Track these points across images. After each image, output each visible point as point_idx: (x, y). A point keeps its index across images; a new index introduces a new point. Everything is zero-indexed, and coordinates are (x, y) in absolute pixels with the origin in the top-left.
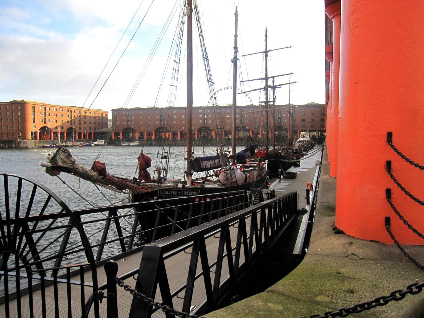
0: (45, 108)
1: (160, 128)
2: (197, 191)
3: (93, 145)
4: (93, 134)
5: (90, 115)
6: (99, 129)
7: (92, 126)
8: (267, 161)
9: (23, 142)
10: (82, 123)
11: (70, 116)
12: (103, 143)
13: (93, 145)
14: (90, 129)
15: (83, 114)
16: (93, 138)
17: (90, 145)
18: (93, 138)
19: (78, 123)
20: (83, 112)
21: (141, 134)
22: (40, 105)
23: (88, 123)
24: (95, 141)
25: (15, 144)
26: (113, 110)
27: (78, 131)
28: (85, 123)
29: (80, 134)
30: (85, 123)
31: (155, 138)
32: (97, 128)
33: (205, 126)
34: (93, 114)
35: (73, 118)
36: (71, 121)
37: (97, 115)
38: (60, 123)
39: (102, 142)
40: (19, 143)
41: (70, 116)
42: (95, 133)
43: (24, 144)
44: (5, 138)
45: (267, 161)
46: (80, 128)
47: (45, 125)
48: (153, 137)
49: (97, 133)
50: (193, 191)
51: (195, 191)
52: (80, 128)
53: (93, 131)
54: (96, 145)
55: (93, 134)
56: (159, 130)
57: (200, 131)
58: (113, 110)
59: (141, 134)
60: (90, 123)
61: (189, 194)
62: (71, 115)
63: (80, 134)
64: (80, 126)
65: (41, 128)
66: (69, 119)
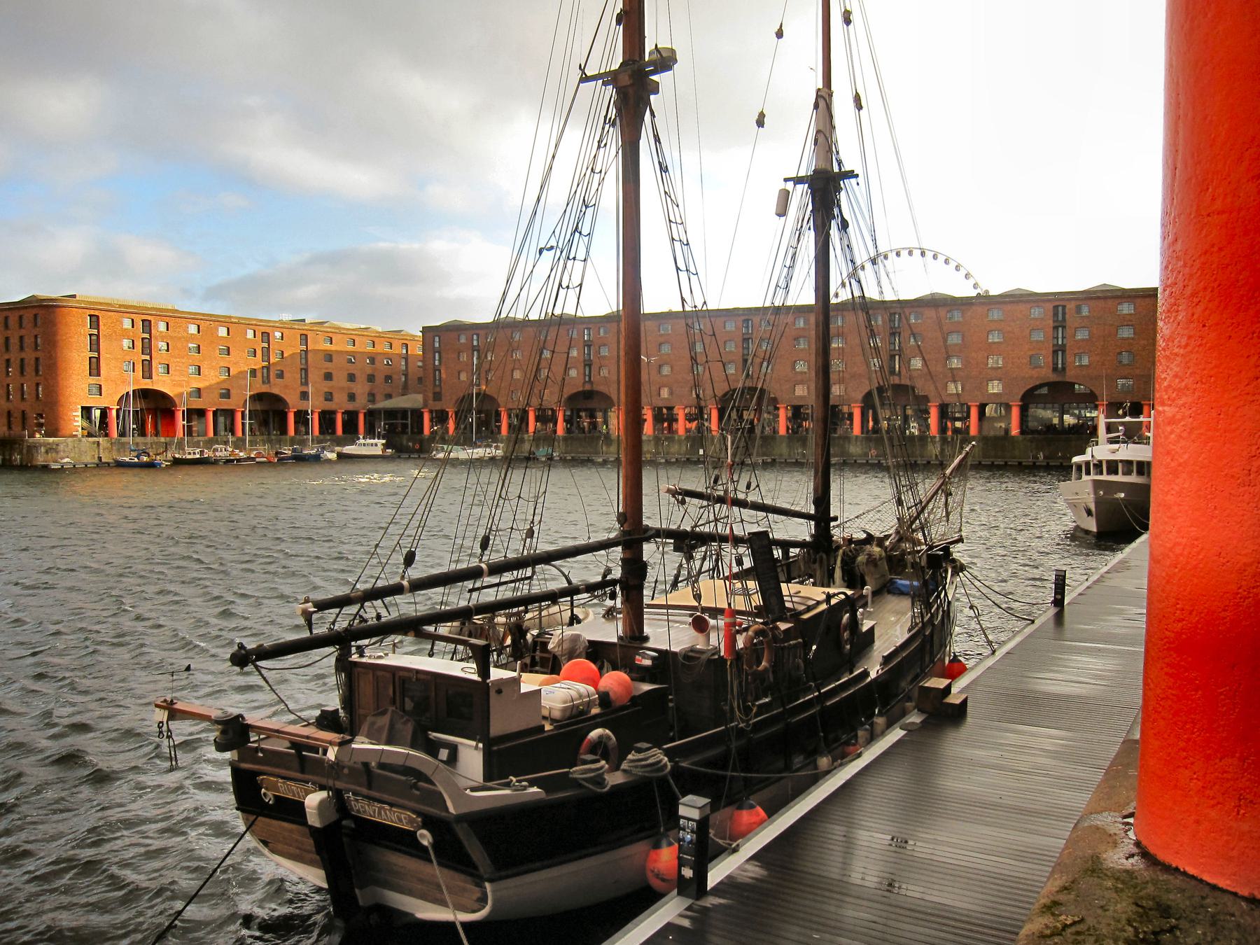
0: (147, 325)
4: (361, 417)
6: (389, 396)
9: (45, 444)
10: (315, 376)
11: (259, 353)
12: (378, 451)
13: (332, 456)
14: (352, 397)
17: (316, 458)
22: (125, 310)
25: (21, 453)
26: (426, 330)
28: (328, 376)
30: (328, 376)
31: (569, 431)
32: (378, 397)
34: (364, 347)
37: (383, 348)
38: (212, 377)
39: (375, 446)
40: (33, 448)
41: (259, 353)
43: (47, 452)
46: (304, 395)
47: (147, 384)
49: (378, 411)
53: (361, 405)
54: (341, 456)
55: (361, 417)
56: (586, 403)
58: (426, 330)
60: (352, 378)
64: (304, 389)
66: (258, 363)
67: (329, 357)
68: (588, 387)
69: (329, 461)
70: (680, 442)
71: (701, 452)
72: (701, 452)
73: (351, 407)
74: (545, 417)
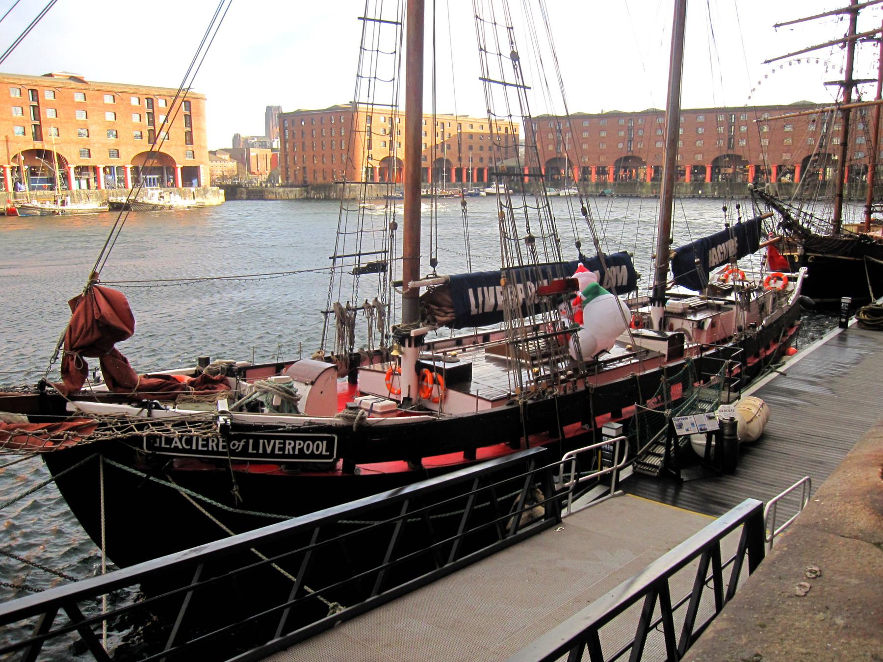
1: (626, 158)
2: (322, 439)
3: (483, 194)
5: (481, 131)
7: (486, 154)
8: (803, 270)
13: (483, 194)
14: (481, 160)
15: (466, 129)
16: (485, 180)
17: (477, 195)
18: (485, 180)
19: (455, 148)
20: (468, 125)
21: (585, 171)
23: (476, 147)
24: (489, 186)
25: (336, 191)
27: (455, 164)
28: (471, 148)
29: (459, 171)
30: (471, 148)
31: (615, 180)
33: (730, 152)
35: (446, 138)
36: (443, 144)
42: (490, 169)
44: (320, 180)
45: (803, 270)
46: (460, 159)
48: (610, 178)
50: (304, 439)
51: (314, 440)
52: (460, 159)
53: (486, 164)
54: (488, 194)
57: (716, 165)
59: (585, 171)
60: (481, 148)
61: (282, 449)
62: (443, 132)
63: (459, 171)
65: (384, 160)
67: (471, 136)
68: (630, 154)
69: (483, 196)
70: (686, 186)
71: (700, 192)
72: (700, 192)
73: (481, 166)
74: (601, 171)
